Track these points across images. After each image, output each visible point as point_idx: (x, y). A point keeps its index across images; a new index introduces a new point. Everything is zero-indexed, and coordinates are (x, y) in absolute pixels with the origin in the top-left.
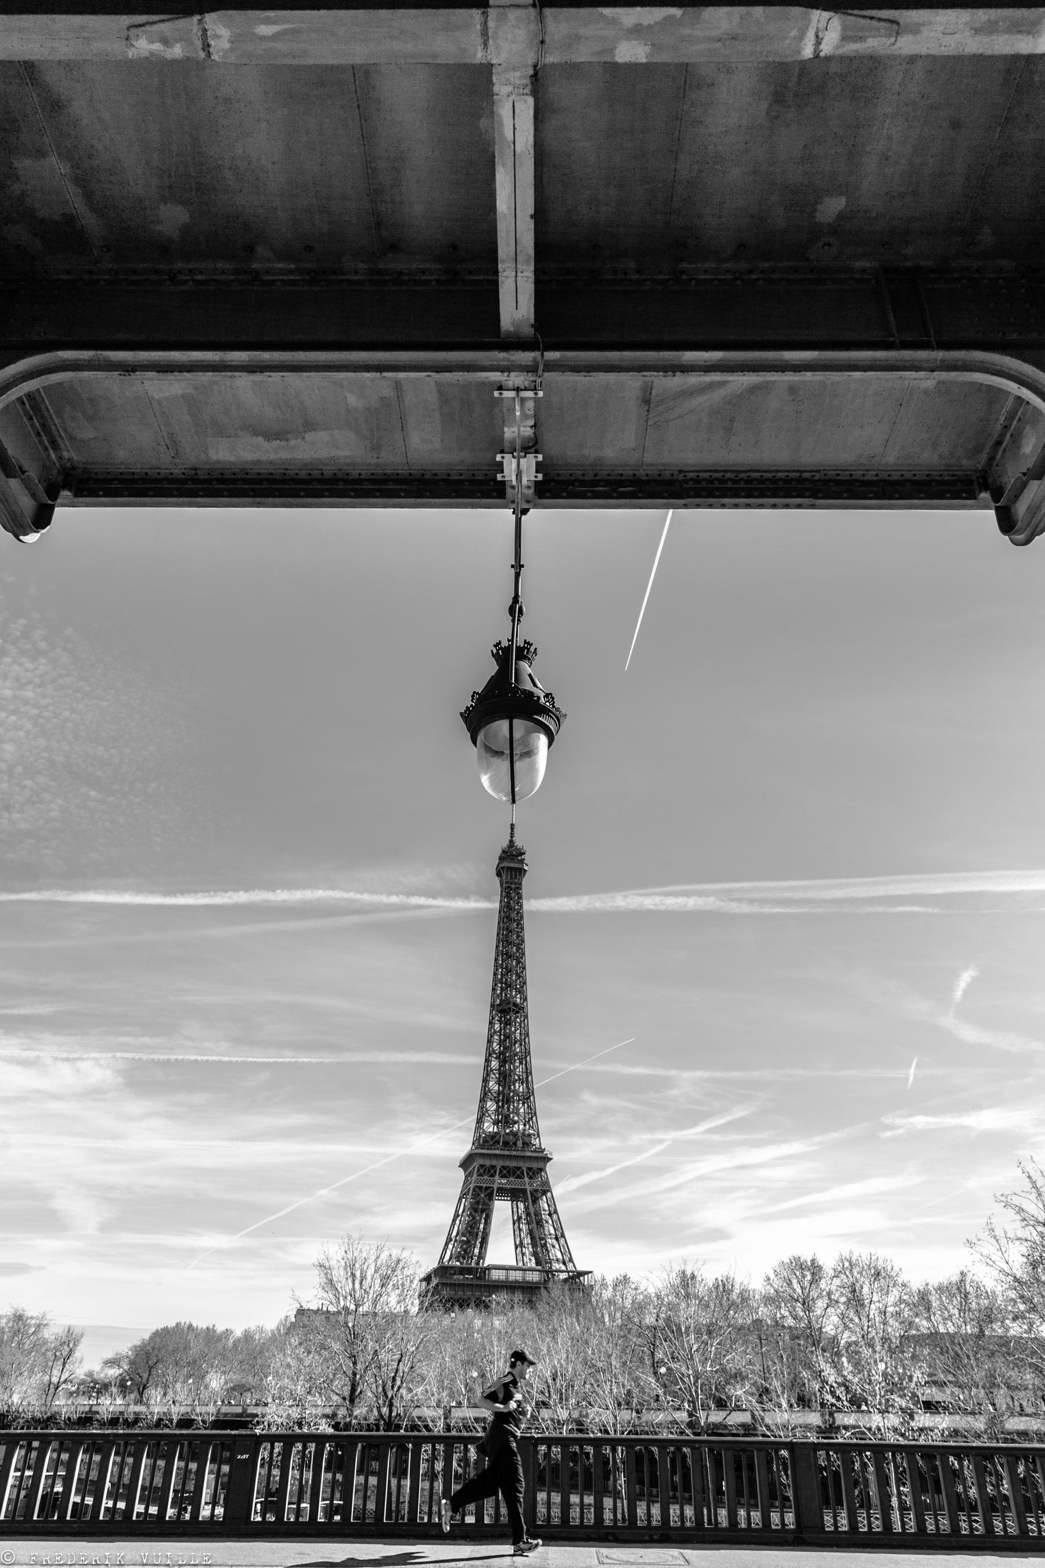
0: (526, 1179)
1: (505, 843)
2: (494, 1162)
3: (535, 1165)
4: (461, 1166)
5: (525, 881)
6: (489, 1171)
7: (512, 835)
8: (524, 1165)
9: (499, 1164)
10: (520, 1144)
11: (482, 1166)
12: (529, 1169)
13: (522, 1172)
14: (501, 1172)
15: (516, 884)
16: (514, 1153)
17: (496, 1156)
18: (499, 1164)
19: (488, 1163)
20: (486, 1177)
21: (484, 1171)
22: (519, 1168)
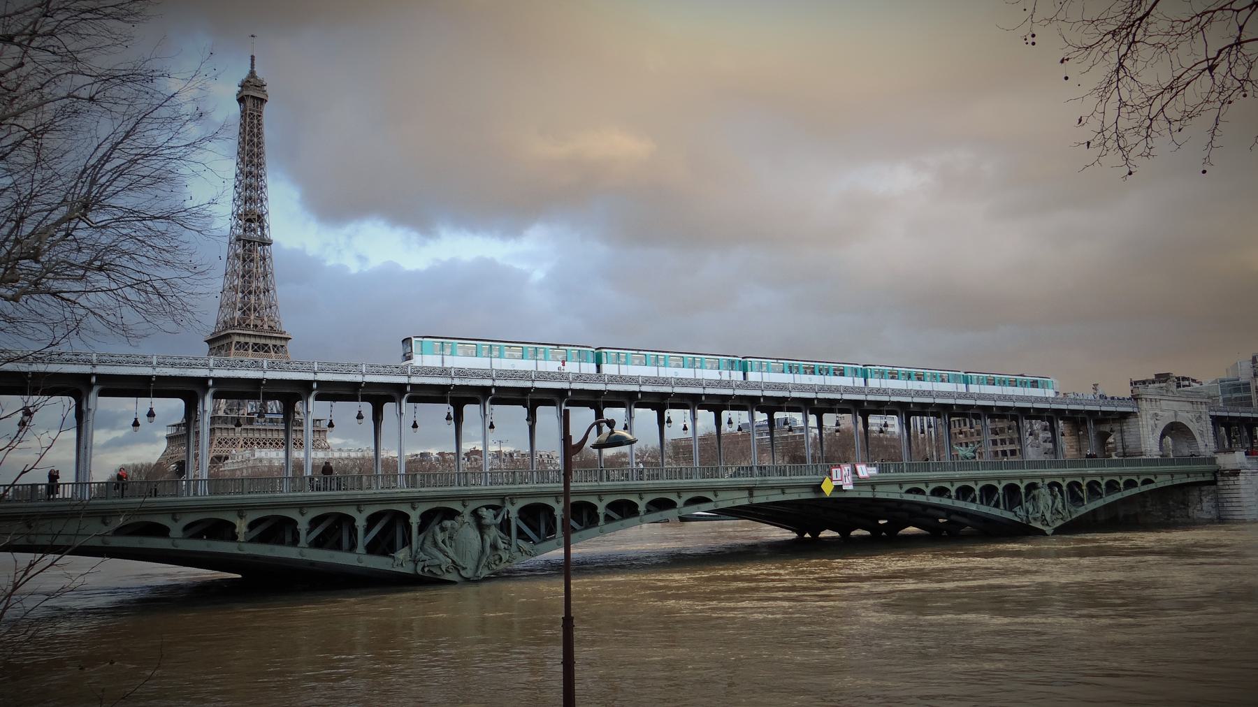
0: (273, 353)
1: (244, 74)
2: (247, 340)
3: (278, 343)
4: (209, 342)
5: (267, 110)
6: (244, 347)
7: (252, 65)
8: (270, 343)
9: (252, 341)
10: (266, 327)
11: (238, 343)
12: (275, 346)
13: (269, 348)
14: (253, 348)
15: (257, 112)
16: (263, 334)
17: (250, 335)
18: (252, 341)
19: (242, 340)
20: (242, 351)
21: (240, 346)
22: (266, 345)
